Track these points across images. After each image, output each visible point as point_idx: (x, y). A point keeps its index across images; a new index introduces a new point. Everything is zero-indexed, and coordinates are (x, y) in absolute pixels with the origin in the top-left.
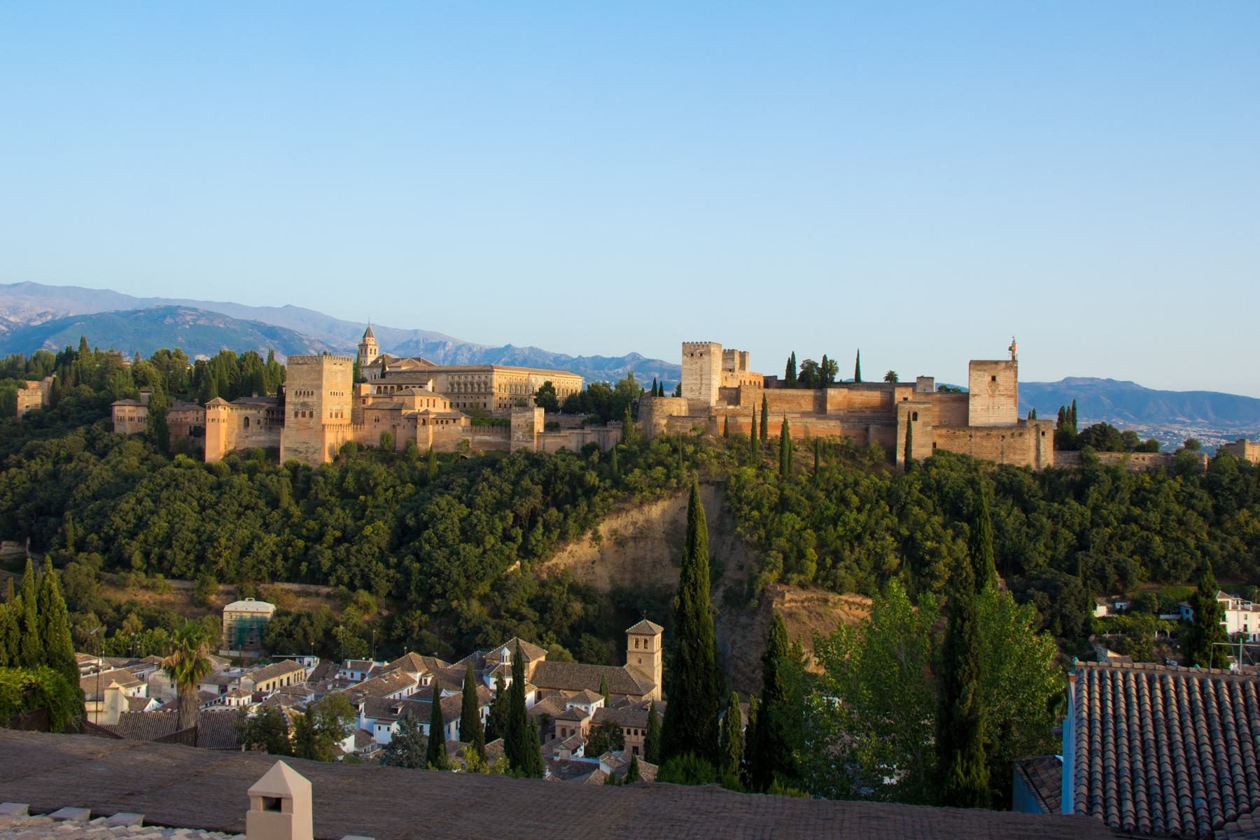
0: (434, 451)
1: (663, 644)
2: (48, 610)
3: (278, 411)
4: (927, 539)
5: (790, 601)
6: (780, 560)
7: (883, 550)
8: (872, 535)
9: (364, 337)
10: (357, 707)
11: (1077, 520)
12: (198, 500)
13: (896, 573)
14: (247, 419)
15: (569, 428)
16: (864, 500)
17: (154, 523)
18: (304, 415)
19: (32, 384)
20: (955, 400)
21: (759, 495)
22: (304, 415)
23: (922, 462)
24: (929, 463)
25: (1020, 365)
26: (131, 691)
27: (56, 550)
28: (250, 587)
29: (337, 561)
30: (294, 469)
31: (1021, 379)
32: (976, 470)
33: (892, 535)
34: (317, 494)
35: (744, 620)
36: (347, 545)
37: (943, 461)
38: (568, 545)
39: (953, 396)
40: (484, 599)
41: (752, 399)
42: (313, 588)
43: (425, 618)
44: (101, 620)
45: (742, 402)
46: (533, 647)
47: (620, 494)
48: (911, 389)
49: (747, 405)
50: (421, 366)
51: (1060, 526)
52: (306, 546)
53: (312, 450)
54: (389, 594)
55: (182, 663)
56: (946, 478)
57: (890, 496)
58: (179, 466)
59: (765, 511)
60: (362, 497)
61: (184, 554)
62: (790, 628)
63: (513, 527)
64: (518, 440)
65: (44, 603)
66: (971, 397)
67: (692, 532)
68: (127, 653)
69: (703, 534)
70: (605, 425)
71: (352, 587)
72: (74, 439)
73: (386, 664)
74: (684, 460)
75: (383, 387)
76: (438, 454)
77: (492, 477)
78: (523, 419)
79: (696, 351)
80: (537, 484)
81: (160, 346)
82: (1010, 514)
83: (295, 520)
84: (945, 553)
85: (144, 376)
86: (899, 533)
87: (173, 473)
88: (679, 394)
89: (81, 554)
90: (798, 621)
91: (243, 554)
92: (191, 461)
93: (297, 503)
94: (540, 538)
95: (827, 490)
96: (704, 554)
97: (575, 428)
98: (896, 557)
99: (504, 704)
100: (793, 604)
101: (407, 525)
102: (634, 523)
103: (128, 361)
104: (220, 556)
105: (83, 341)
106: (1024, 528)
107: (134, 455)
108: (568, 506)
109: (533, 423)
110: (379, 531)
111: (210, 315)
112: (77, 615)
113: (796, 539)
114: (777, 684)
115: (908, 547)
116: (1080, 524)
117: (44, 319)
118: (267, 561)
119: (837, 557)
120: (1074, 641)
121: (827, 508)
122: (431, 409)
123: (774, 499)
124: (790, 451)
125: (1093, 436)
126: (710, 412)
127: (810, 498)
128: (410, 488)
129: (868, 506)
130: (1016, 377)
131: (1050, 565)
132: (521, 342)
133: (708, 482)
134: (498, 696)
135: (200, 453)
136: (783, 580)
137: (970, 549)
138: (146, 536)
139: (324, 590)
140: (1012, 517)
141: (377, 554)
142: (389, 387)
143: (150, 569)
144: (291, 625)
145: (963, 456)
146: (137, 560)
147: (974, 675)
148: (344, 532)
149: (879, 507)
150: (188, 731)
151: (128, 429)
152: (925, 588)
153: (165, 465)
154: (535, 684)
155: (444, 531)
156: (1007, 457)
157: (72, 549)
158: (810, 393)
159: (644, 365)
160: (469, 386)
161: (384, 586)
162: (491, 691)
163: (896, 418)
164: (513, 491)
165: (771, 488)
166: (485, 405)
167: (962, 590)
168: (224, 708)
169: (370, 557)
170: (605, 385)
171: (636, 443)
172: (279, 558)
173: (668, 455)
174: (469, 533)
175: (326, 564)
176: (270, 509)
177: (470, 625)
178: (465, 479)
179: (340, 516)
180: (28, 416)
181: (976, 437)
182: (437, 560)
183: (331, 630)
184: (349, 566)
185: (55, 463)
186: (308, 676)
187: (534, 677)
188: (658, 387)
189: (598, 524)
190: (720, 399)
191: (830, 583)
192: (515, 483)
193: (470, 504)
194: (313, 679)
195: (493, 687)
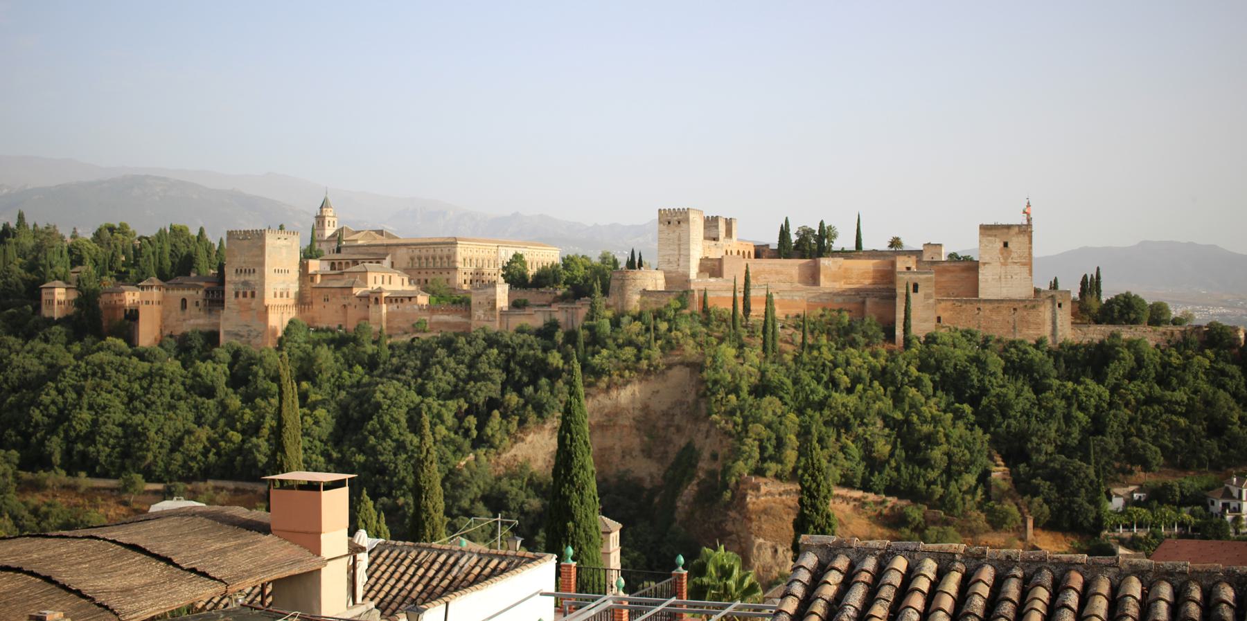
3: (218, 292)
5: (766, 495)
14: (184, 301)
16: (856, 380)
18: (245, 295)
22: (245, 295)
23: (923, 339)
24: (930, 339)
28: (181, 486)
30: (236, 355)
41: (734, 272)
42: (248, 486)
48: (914, 258)
53: (255, 333)
57: (883, 376)
59: (744, 394)
64: (479, 319)
74: (656, 339)
75: (336, 262)
78: (485, 296)
91: (172, 450)
97: (545, 305)
122: (386, 287)
125: (1116, 308)
129: (860, 387)
130: (1031, 242)
135: (131, 339)
142: (344, 262)
145: (968, 331)
151: (57, 313)
160: (431, 260)
163: (895, 290)
166: (448, 280)
173: (638, 335)
190: (701, 271)
192: (471, 366)
193: (421, 391)
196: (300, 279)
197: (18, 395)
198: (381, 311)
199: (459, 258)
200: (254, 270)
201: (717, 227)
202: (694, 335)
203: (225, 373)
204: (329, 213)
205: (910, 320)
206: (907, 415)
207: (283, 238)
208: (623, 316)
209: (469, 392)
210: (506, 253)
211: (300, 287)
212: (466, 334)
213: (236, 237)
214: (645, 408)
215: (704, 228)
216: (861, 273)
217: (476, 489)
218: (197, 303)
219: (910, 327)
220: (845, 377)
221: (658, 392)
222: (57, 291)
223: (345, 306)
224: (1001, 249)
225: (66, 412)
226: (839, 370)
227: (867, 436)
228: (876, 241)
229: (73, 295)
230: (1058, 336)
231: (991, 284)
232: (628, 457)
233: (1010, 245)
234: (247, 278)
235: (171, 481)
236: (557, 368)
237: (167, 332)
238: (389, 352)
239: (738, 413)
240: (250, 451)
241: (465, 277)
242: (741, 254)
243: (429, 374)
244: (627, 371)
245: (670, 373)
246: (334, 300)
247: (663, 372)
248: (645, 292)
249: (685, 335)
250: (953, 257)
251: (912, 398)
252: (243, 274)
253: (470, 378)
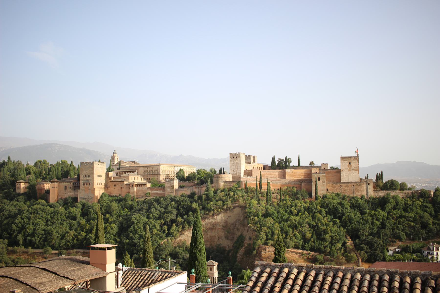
5: (268, 252)
14: (66, 187)
16: (299, 211)
18: (87, 184)
22: (87, 184)
23: (322, 197)
24: (324, 197)
28: (65, 251)
30: (84, 205)
41: (256, 174)
53: (90, 198)
57: (308, 210)
59: (260, 217)
74: (229, 198)
75: (119, 173)
78: (170, 184)
91: (61, 239)
97: (191, 187)
102: (210, 223)
109: (174, 185)
122: (136, 181)
125: (388, 185)
129: (300, 214)
130: (358, 162)
135: (47, 200)
142: (121, 173)
145: (337, 194)
151: (22, 191)
160: (151, 172)
173: (223, 197)
190: (245, 174)
193: (148, 217)
196: (106, 179)
197: (7, 220)
199: (161, 171)
201: (250, 159)
202: (242, 197)
203: (80, 212)
204: (116, 156)
205: (317, 190)
206: (317, 223)
207: (100, 165)
208: (218, 190)
209: (165, 217)
210: (177, 169)
211: (106, 181)
212: (163, 197)
213: (84, 164)
214: (226, 222)
215: (246, 159)
216: (300, 174)
217: (167, 251)
218: (70, 187)
221: (230, 216)
222: (21, 184)
223: (121, 188)
224: (348, 165)
225: (24, 226)
226: (293, 208)
227: (303, 231)
228: (305, 163)
229: (27, 185)
230: (368, 195)
231: (345, 177)
232: (220, 239)
235: (61, 250)
237: (60, 198)
238: (137, 204)
239: (258, 224)
240: (89, 239)
241: (163, 177)
242: (259, 168)
243: (151, 211)
245: (235, 210)
246: (118, 186)
247: (232, 210)
248: (225, 182)
249: (239, 197)
250: (332, 168)
253: (165, 212)
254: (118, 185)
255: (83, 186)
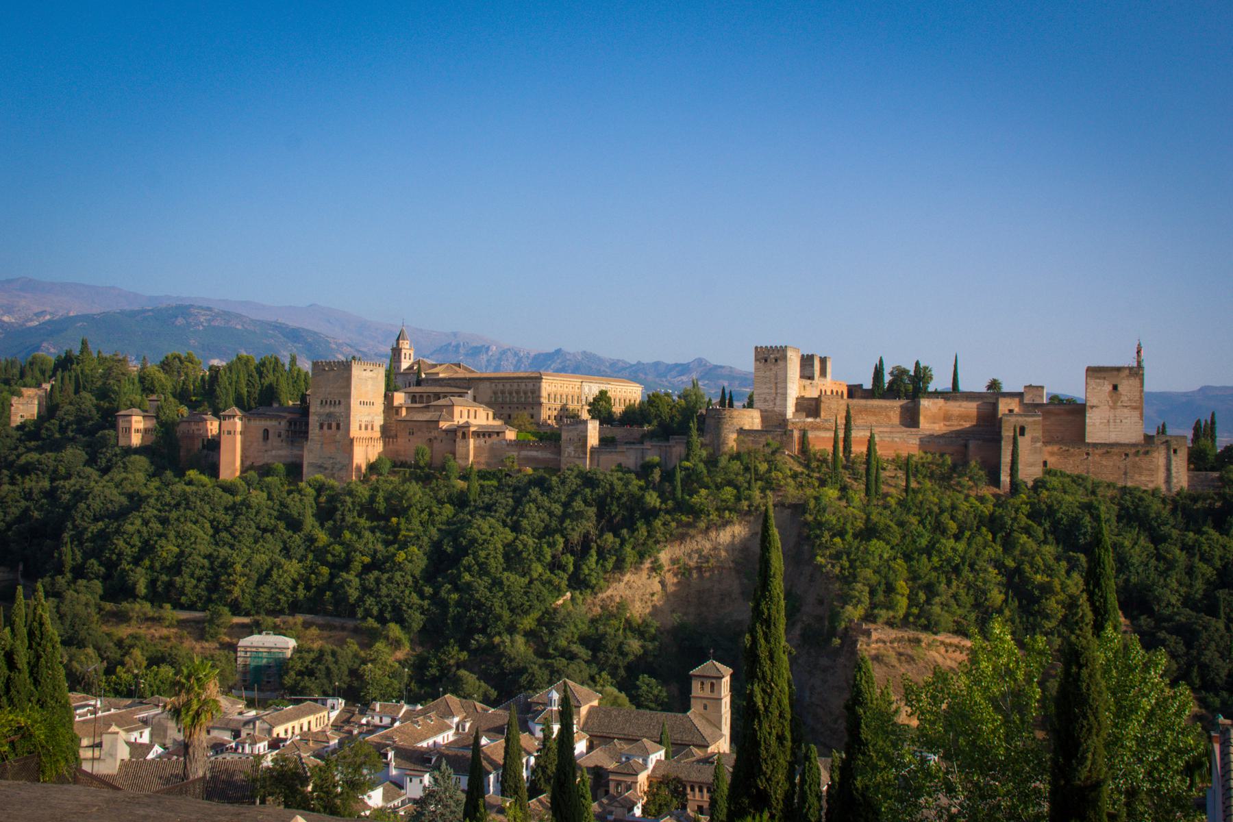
0: (476, 468)
1: (732, 689)
2: (39, 645)
4: (1036, 573)
5: (877, 642)
6: (866, 594)
7: (985, 584)
8: (972, 566)
9: (398, 340)
10: (386, 756)
11: (1218, 552)
12: (211, 522)
13: (1000, 611)
14: (266, 431)
15: (626, 443)
17: (162, 547)
18: (330, 427)
19: (28, 392)
20: (1070, 412)
21: (842, 520)
22: (330, 427)
23: (1030, 484)
24: (1038, 485)
25: (1146, 372)
26: (134, 736)
27: (52, 577)
28: (270, 620)
29: (365, 590)
30: (320, 489)
31: (1148, 388)
32: (1093, 493)
33: (995, 567)
34: (343, 514)
35: (824, 661)
36: (376, 573)
37: (1054, 482)
38: (623, 574)
39: (1067, 407)
40: (530, 635)
41: (834, 411)
42: (337, 621)
43: (464, 655)
44: (100, 656)
45: (822, 414)
46: (585, 689)
47: (684, 518)
48: (1017, 400)
49: (828, 417)
50: (461, 374)
51: (1196, 559)
52: (331, 574)
53: (339, 466)
54: (423, 630)
55: (188, 705)
56: (1059, 502)
57: (994, 523)
58: (190, 483)
59: (849, 537)
60: (394, 520)
61: (194, 582)
62: (877, 672)
63: (563, 554)
65: (35, 635)
66: (1087, 408)
67: (765, 563)
68: (131, 692)
69: (777, 562)
70: (668, 440)
71: (382, 620)
72: (73, 455)
73: (419, 707)
75: (417, 395)
76: (479, 471)
77: (540, 498)
78: (575, 433)
79: (771, 357)
80: (590, 505)
81: (171, 349)
82: (1136, 543)
83: (320, 544)
84: (1058, 588)
85: (152, 383)
86: (1003, 563)
87: (184, 492)
88: (750, 405)
89: (80, 582)
90: (886, 665)
92: (205, 479)
93: (322, 525)
94: (594, 566)
95: (920, 514)
96: (778, 586)
97: (633, 443)
98: (1001, 592)
99: (551, 754)
100: (880, 644)
101: (445, 551)
102: (699, 552)
103: (134, 367)
104: (235, 583)
105: (84, 343)
106: (1153, 562)
107: (140, 470)
108: (624, 531)
109: (586, 437)
110: (415, 559)
111: (226, 314)
112: (74, 649)
113: (884, 570)
114: (863, 736)
115: (1015, 582)
116: (1221, 558)
117: (42, 320)
118: (287, 590)
119: (930, 590)
120: (1217, 695)
121: (920, 536)
122: (472, 421)
123: (860, 524)
124: (877, 470)
126: (786, 425)
127: (901, 524)
128: (449, 510)
129: (967, 534)
131: (1185, 604)
132: (573, 346)
133: (783, 505)
134: (544, 745)
135: (213, 470)
136: (870, 617)
137: (1087, 583)
138: (152, 561)
139: (351, 624)
140: (1137, 547)
141: (410, 583)
142: (425, 395)
143: (157, 596)
144: (312, 662)
145: (1078, 477)
146: (142, 589)
147: (1094, 731)
148: (373, 557)
149: (981, 534)
150: (194, 781)
151: (136, 440)
152: (1032, 629)
153: (175, 483)
154: (587, 732)
155: (487, 558)
156: (1132, 478)
157: (69, 575)
158: (898, 403)
159: (712, 372)
161: (417, 620)
162: (537, 739)
163: (999, 433)
164: (564, 512)
165: (856, 511)
167: (1078, 632)
168: (236, 756)
169: (402, 587)
170: (667, 394)
171: (701, 461)
172: (301, 587)
174: (513, 558)
175: (353, 594)
176: (290, 533)
177: (514, 664)
178: (510, 500)
179: (370, 542)
180: (21, 427)
181: (1094, 454)
182: (477, 592)
183: (357, 669)
184: (380, 596)
185: (52, 480)
186: (332, 720)
187: (586, 723)
188: (727, 397)
189: (659, 551)
190: (797, 411)
191: (923, 621)
192: (566, 505)
193: (516, 528)
194: (337, 727)
195: (539, 734)
196: (384, 412)
198: (468, 446)
200: (340, 402)
201: (812, 365)
211: (385, 420)
217: (573, 628)
219: (1017, 471)
220: (951, 522)
222: (134, 418)
224: (1110, 392)
225: (152, 542)
227: (978, 583)
229: (151, 424)
233: (1120, 388)
234: (332, 409)
235: (258, 613)
236: (655, 507)
237: (248, 463)
239: (845, 557)
243: (523, 512)
244: (727, 512)
246: (419, 433)
248: (741, 431)
251: (1023, 545)
252: (327, 406)
254: (419, 430)
255: (317, 430)
